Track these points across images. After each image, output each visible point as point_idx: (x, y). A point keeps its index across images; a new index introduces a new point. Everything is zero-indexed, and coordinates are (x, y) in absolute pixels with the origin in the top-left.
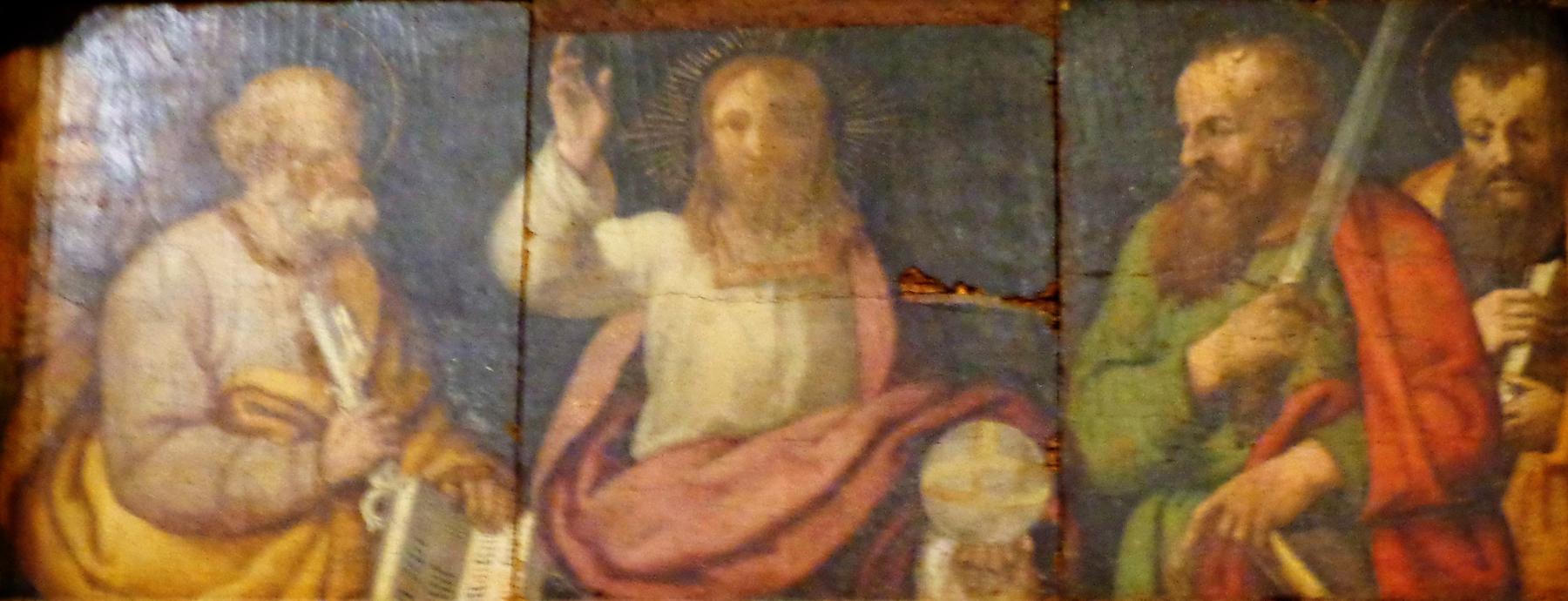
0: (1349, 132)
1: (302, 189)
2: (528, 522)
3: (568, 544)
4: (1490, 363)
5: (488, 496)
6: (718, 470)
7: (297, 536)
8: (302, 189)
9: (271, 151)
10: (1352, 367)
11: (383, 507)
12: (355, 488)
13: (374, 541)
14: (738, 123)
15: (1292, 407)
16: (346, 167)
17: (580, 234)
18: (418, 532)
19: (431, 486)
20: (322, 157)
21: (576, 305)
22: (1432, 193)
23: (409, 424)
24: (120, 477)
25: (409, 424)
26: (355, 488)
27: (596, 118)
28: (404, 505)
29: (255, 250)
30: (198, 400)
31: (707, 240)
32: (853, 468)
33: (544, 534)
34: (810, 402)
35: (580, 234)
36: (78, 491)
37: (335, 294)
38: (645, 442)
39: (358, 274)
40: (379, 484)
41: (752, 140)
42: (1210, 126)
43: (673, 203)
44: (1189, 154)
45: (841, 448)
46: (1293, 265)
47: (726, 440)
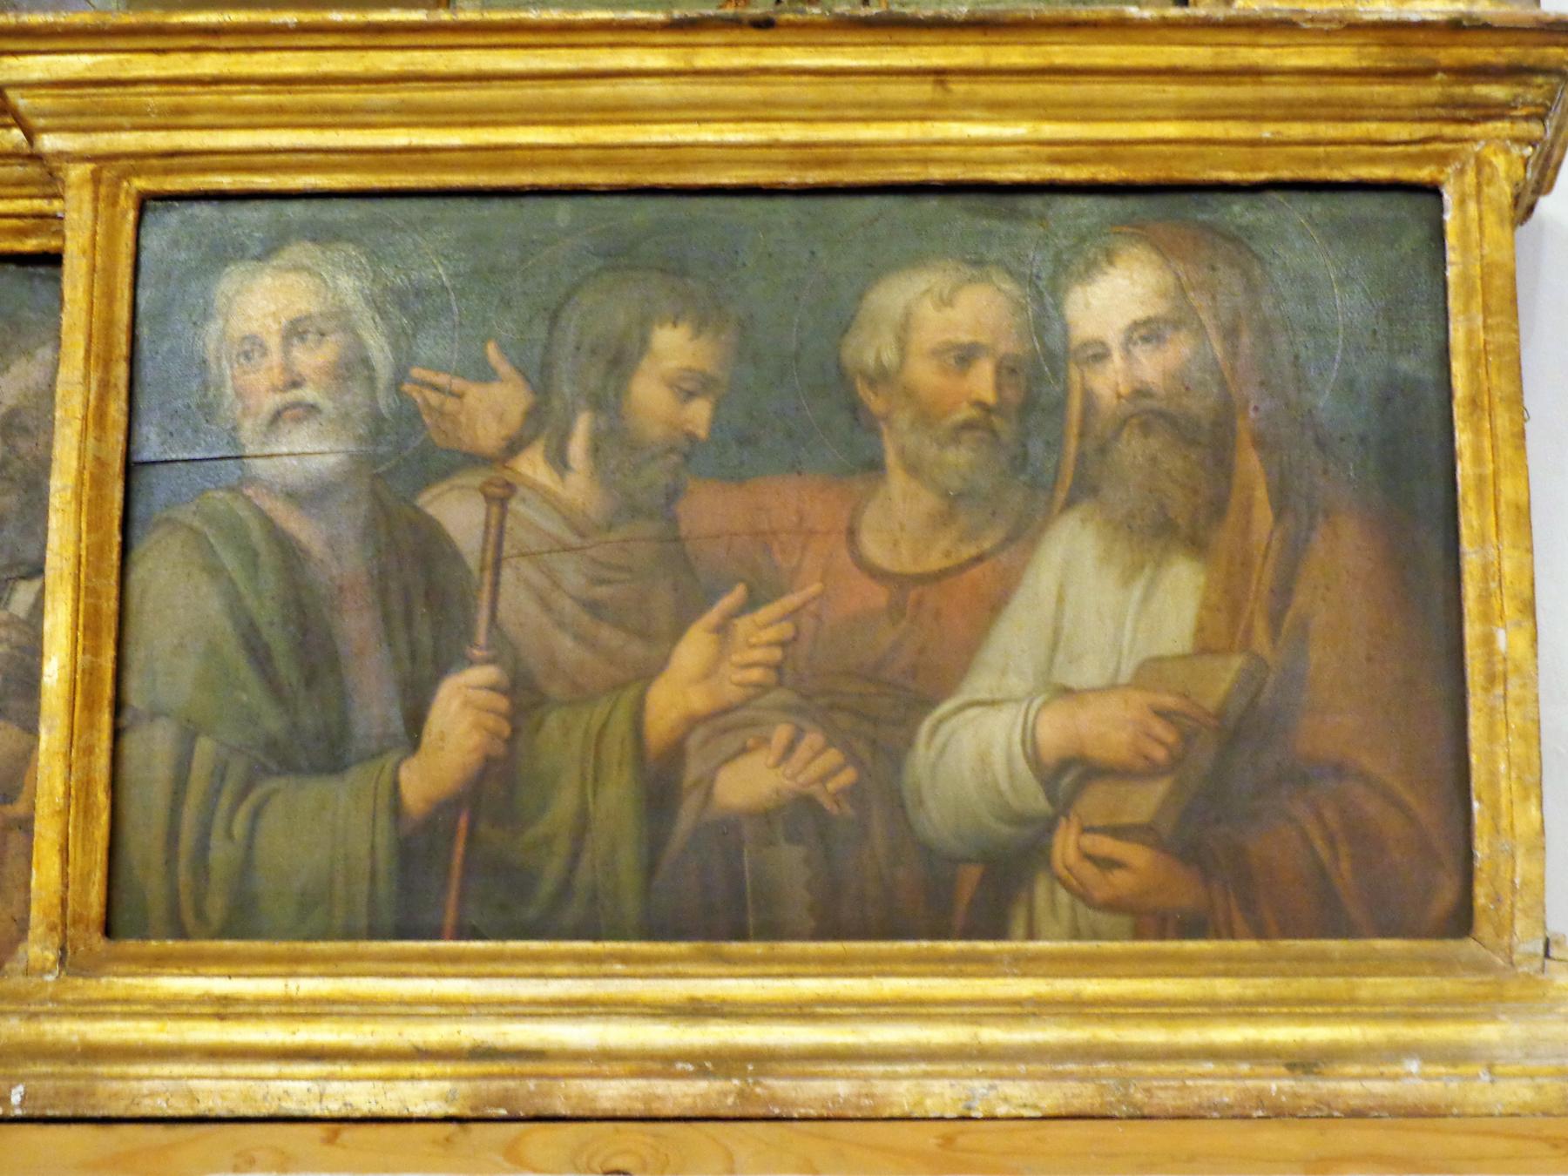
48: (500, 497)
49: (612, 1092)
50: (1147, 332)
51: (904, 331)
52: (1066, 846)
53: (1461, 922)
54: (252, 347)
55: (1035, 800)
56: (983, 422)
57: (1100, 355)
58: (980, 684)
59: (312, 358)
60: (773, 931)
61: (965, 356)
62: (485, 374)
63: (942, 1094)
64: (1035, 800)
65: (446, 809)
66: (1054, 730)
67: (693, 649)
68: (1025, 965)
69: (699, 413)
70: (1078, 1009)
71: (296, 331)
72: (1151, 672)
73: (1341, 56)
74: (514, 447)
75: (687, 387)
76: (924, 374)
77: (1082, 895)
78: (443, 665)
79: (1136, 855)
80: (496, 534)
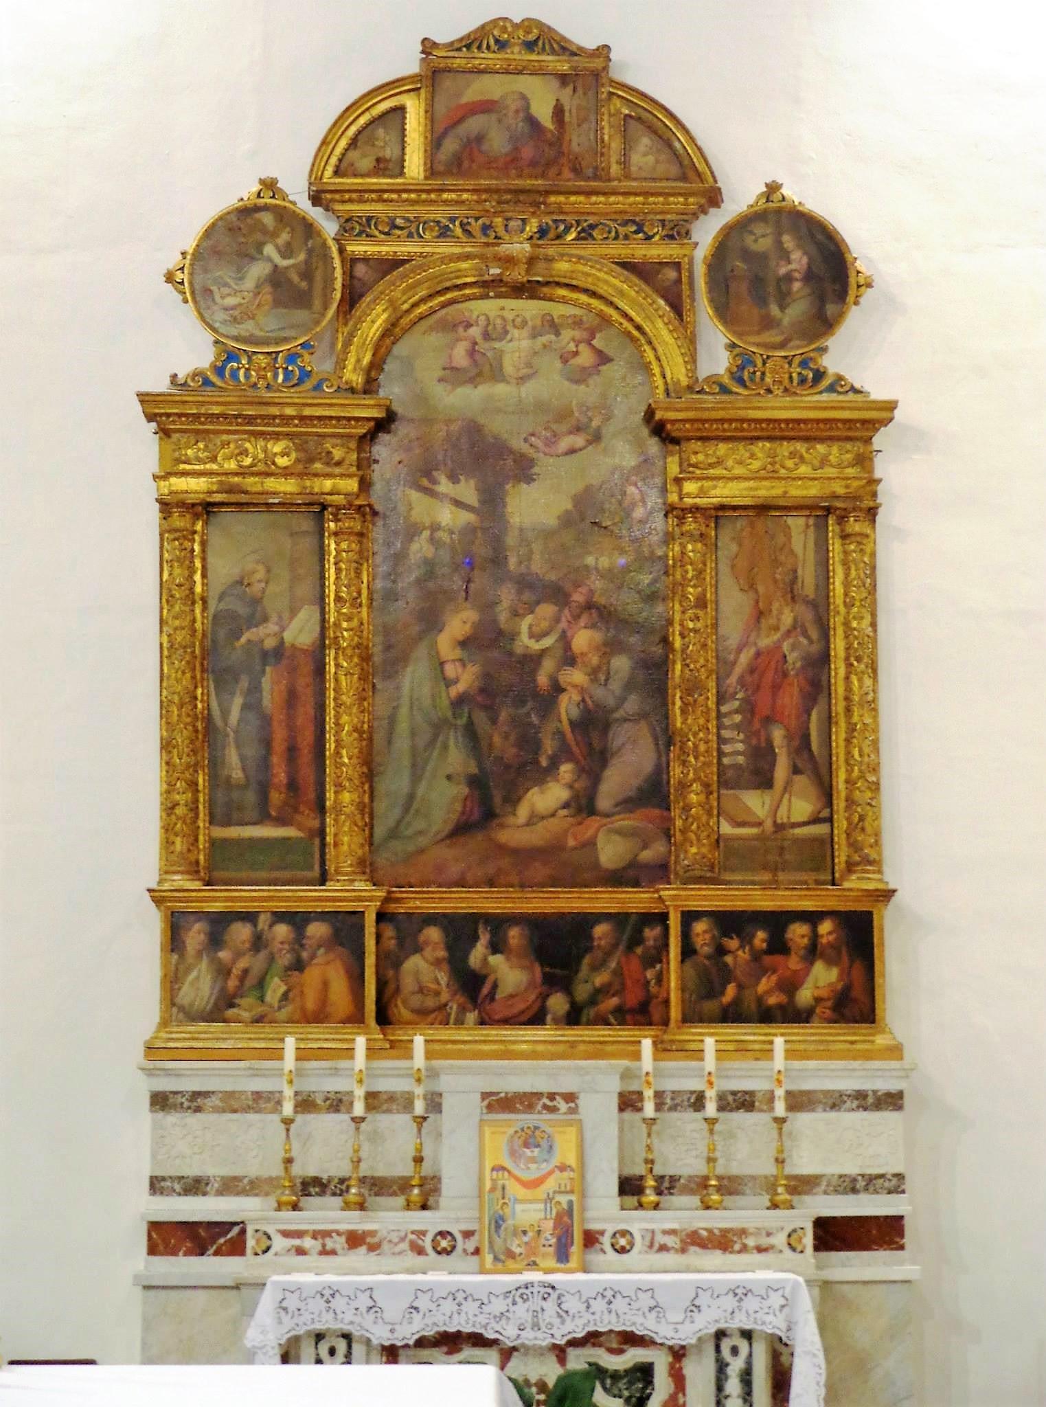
0: (625, 937)
1: (434, 950)
2: (476, 1012)
3: (483, 1014)
4: (648, 982)
5: (470, 1006)
6: (510, 1003)
7: (436, 1013)
8: (434, 950)
9: (427, 943)
10: (623, 985)
11: (451, 1008)
12: (446, 1005)
13: (449, 1015)
14: (513, 937)
15: (612, 992)
16: (442, 946)
17: (485, 960)
18: (457, 1014)
19: (459, 1005)
20: (436, 943)
21: (484, 972)
22: (639, 950)
23: (455, 994)
24: (405, 1002)
25: (455, 994)
26: (446, 1005)
27: (488, 936)
28: (455, 1007)
29: (427, 961)
30: (416, 989)
31: (508, 959)
32: (533, 1002)
33: (480, 1012)
34: (526, 989)
35: (485, 960)
36: (396, 1006)
37: (440, 970)
38: (497, 997)
39: (446, 966)
40: (450, 1004)
41: (516, 941)
42: (600, 938)
43: (501, 952)
44: (595, 944)
45: (532, 997)
46: (613, 965)
47: (512, 996)
48: (736, 957)
49: (757, 1047)
50: (830, 933)
51: (794, 930)
52: (818, 1010)
53: (873, 1022)
54: (698, 935)
55: (813, 1003)
56: (805, 948)
57: (822, 936)
58: (805, 986)
59: (707, 936)
60: (776, 1022)
61: (803, 936)
62: (732, 938)
63: (802, 1047)
64: (813, 1003)
65: (730, 1005)
66: (817, 993)
67: (764, 980)
68: (812, 1027)
69: (765, 945)
70: (821, 1034)
71: (705, 932)
72: (830, 985)
73: (860, 894)
74: (738, 950)
75: (763, 941)
76: (798, 940)
77: (820, 1018)
78: (729, 983)
79: (828, 1011)
80: (735, 963)
